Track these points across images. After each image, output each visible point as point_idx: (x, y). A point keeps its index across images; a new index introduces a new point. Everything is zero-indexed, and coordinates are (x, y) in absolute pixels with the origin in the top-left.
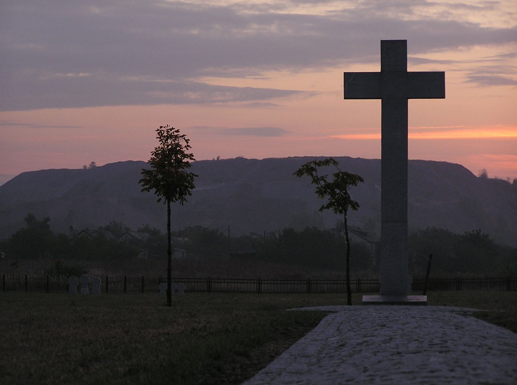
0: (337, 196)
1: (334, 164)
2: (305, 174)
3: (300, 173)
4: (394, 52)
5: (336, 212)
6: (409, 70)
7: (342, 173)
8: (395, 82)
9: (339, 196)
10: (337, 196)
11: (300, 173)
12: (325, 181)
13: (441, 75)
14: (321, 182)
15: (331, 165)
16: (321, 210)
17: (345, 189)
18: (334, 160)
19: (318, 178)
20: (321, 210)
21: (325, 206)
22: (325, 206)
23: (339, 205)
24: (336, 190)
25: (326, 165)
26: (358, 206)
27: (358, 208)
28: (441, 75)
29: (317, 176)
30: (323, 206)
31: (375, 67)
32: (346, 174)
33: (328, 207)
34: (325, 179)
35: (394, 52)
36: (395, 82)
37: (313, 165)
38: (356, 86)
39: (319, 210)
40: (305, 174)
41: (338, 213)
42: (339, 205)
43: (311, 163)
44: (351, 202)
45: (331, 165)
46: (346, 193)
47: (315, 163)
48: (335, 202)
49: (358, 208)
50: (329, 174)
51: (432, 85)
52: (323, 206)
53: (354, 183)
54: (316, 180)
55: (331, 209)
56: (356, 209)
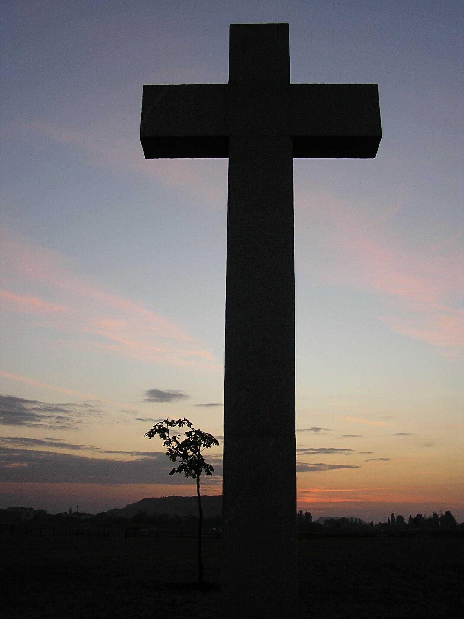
0: (189, 459)
1: (188, 426)
2: (157, 435)
3: (151, 434)
4: (259, 48)
5: (187, 476)
6: (294, 79)
7: (195, 431)
8: (262, 126)
9: (192, 459)
10: (189, 459)
11: (151, 434)
12: (178, 442)
13: (365, 98)
14: (172, 443)
15: (185, 426)
16: (172, 473)
17: (198, 450)
18: (188, 422)
19: (169, 439)
20: (172, 473)
21: (176, 470)
22: (176, 470)
23: (191, 469)
24: (188, 452)
25: (180, 426)
26: (212, 469)
27: (212, 472)
28: (365, 98)
29: (168, 437)
30: (174, 469)
31: (216, 71)
32: (198, 432)
33: (180, 470)
34: (177, 439)
35: (259, 48)
36: (262, 126)
37: (165, 425)
38: (173, 125)
39: (170, 474)
40: (157, 435)
41: (190, 477)
42: (191, 469)
43: (162, 423)
44: (206, 465)
45: (185, 426)
46: (199, 455)
47: (167, 422)
48: (186, 466)
49: (212, 472)
50: (181, 434)
51: (348, 125)
52: (174, 469)
53: (208, 446)
54: (168, 443)
55: (183, 472)
56: (211, 474)
